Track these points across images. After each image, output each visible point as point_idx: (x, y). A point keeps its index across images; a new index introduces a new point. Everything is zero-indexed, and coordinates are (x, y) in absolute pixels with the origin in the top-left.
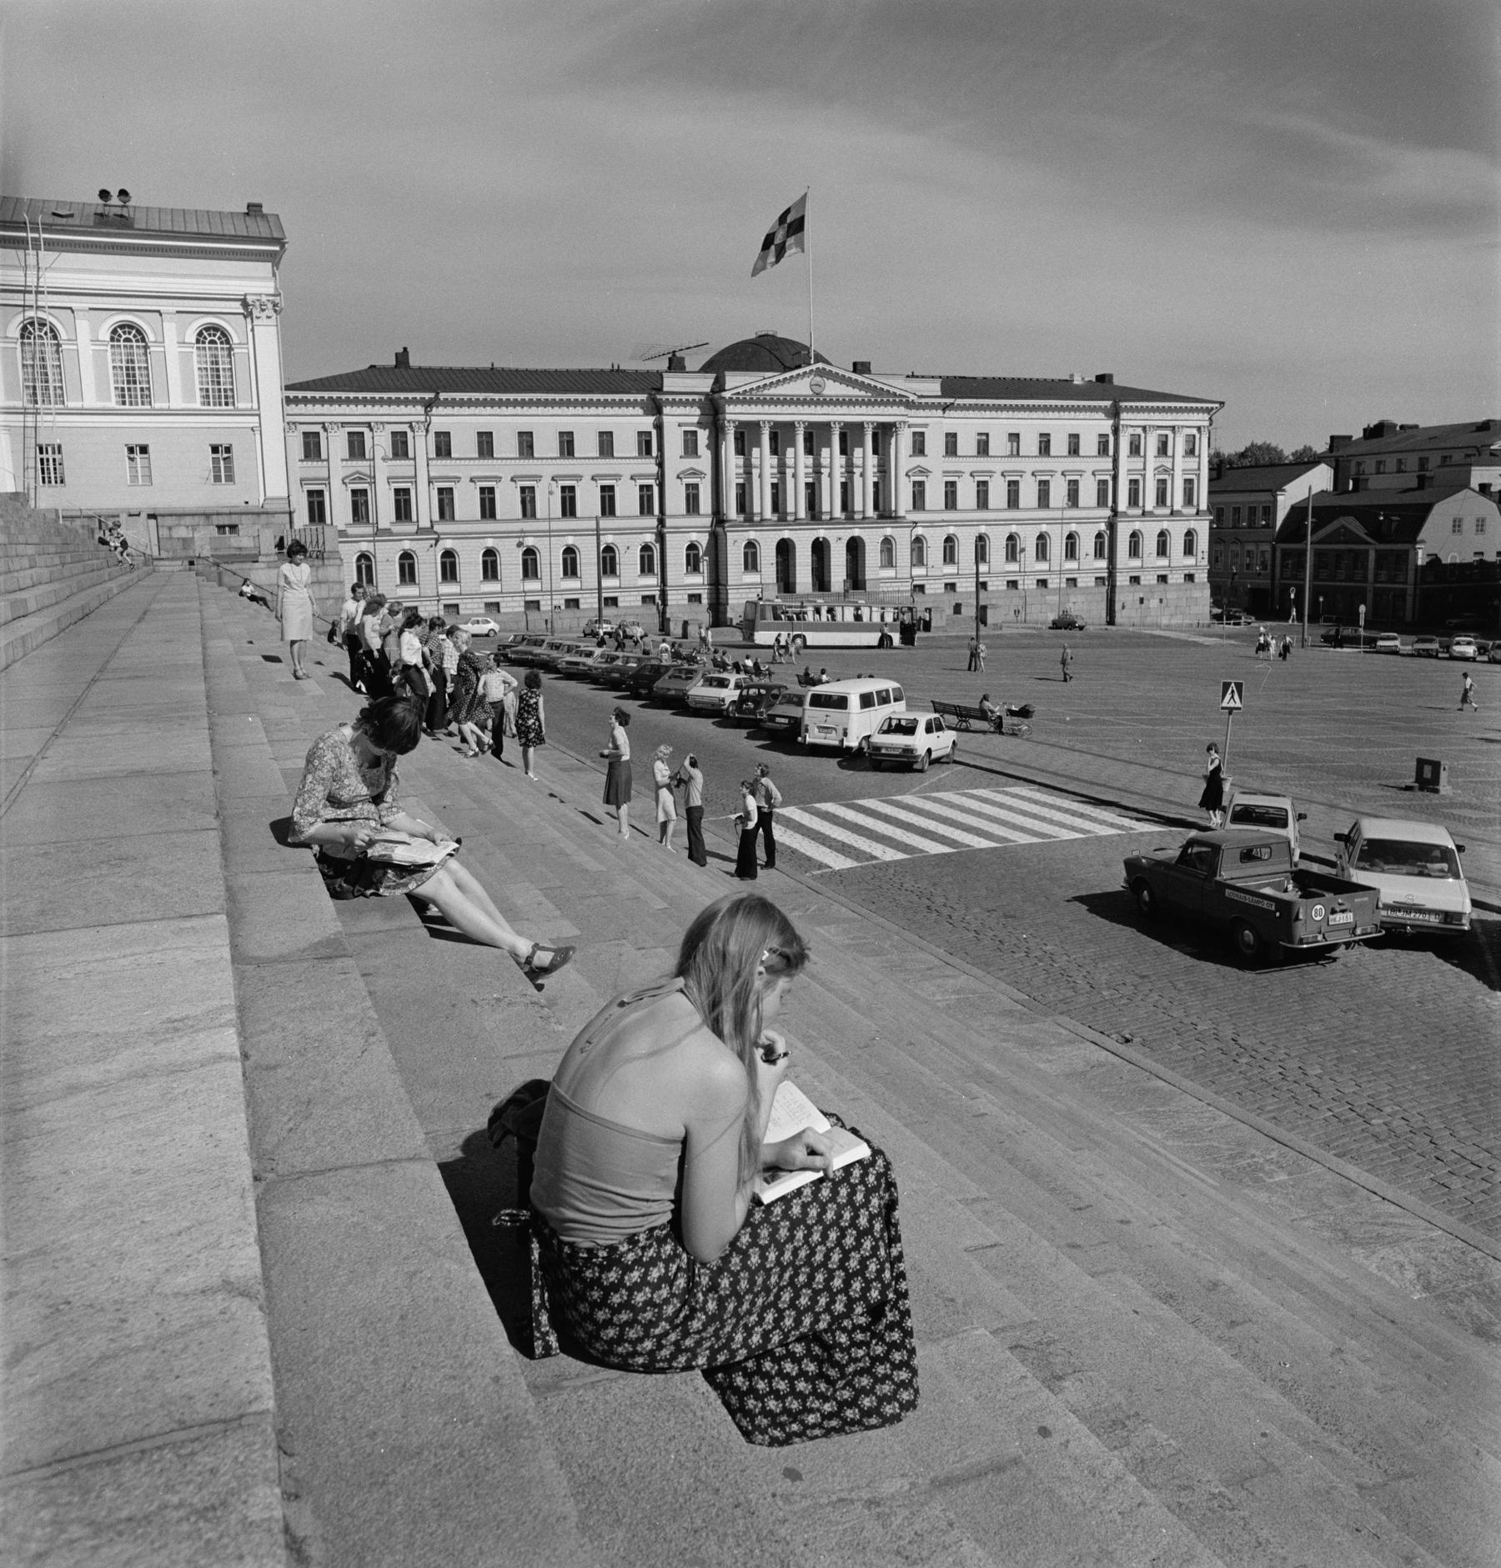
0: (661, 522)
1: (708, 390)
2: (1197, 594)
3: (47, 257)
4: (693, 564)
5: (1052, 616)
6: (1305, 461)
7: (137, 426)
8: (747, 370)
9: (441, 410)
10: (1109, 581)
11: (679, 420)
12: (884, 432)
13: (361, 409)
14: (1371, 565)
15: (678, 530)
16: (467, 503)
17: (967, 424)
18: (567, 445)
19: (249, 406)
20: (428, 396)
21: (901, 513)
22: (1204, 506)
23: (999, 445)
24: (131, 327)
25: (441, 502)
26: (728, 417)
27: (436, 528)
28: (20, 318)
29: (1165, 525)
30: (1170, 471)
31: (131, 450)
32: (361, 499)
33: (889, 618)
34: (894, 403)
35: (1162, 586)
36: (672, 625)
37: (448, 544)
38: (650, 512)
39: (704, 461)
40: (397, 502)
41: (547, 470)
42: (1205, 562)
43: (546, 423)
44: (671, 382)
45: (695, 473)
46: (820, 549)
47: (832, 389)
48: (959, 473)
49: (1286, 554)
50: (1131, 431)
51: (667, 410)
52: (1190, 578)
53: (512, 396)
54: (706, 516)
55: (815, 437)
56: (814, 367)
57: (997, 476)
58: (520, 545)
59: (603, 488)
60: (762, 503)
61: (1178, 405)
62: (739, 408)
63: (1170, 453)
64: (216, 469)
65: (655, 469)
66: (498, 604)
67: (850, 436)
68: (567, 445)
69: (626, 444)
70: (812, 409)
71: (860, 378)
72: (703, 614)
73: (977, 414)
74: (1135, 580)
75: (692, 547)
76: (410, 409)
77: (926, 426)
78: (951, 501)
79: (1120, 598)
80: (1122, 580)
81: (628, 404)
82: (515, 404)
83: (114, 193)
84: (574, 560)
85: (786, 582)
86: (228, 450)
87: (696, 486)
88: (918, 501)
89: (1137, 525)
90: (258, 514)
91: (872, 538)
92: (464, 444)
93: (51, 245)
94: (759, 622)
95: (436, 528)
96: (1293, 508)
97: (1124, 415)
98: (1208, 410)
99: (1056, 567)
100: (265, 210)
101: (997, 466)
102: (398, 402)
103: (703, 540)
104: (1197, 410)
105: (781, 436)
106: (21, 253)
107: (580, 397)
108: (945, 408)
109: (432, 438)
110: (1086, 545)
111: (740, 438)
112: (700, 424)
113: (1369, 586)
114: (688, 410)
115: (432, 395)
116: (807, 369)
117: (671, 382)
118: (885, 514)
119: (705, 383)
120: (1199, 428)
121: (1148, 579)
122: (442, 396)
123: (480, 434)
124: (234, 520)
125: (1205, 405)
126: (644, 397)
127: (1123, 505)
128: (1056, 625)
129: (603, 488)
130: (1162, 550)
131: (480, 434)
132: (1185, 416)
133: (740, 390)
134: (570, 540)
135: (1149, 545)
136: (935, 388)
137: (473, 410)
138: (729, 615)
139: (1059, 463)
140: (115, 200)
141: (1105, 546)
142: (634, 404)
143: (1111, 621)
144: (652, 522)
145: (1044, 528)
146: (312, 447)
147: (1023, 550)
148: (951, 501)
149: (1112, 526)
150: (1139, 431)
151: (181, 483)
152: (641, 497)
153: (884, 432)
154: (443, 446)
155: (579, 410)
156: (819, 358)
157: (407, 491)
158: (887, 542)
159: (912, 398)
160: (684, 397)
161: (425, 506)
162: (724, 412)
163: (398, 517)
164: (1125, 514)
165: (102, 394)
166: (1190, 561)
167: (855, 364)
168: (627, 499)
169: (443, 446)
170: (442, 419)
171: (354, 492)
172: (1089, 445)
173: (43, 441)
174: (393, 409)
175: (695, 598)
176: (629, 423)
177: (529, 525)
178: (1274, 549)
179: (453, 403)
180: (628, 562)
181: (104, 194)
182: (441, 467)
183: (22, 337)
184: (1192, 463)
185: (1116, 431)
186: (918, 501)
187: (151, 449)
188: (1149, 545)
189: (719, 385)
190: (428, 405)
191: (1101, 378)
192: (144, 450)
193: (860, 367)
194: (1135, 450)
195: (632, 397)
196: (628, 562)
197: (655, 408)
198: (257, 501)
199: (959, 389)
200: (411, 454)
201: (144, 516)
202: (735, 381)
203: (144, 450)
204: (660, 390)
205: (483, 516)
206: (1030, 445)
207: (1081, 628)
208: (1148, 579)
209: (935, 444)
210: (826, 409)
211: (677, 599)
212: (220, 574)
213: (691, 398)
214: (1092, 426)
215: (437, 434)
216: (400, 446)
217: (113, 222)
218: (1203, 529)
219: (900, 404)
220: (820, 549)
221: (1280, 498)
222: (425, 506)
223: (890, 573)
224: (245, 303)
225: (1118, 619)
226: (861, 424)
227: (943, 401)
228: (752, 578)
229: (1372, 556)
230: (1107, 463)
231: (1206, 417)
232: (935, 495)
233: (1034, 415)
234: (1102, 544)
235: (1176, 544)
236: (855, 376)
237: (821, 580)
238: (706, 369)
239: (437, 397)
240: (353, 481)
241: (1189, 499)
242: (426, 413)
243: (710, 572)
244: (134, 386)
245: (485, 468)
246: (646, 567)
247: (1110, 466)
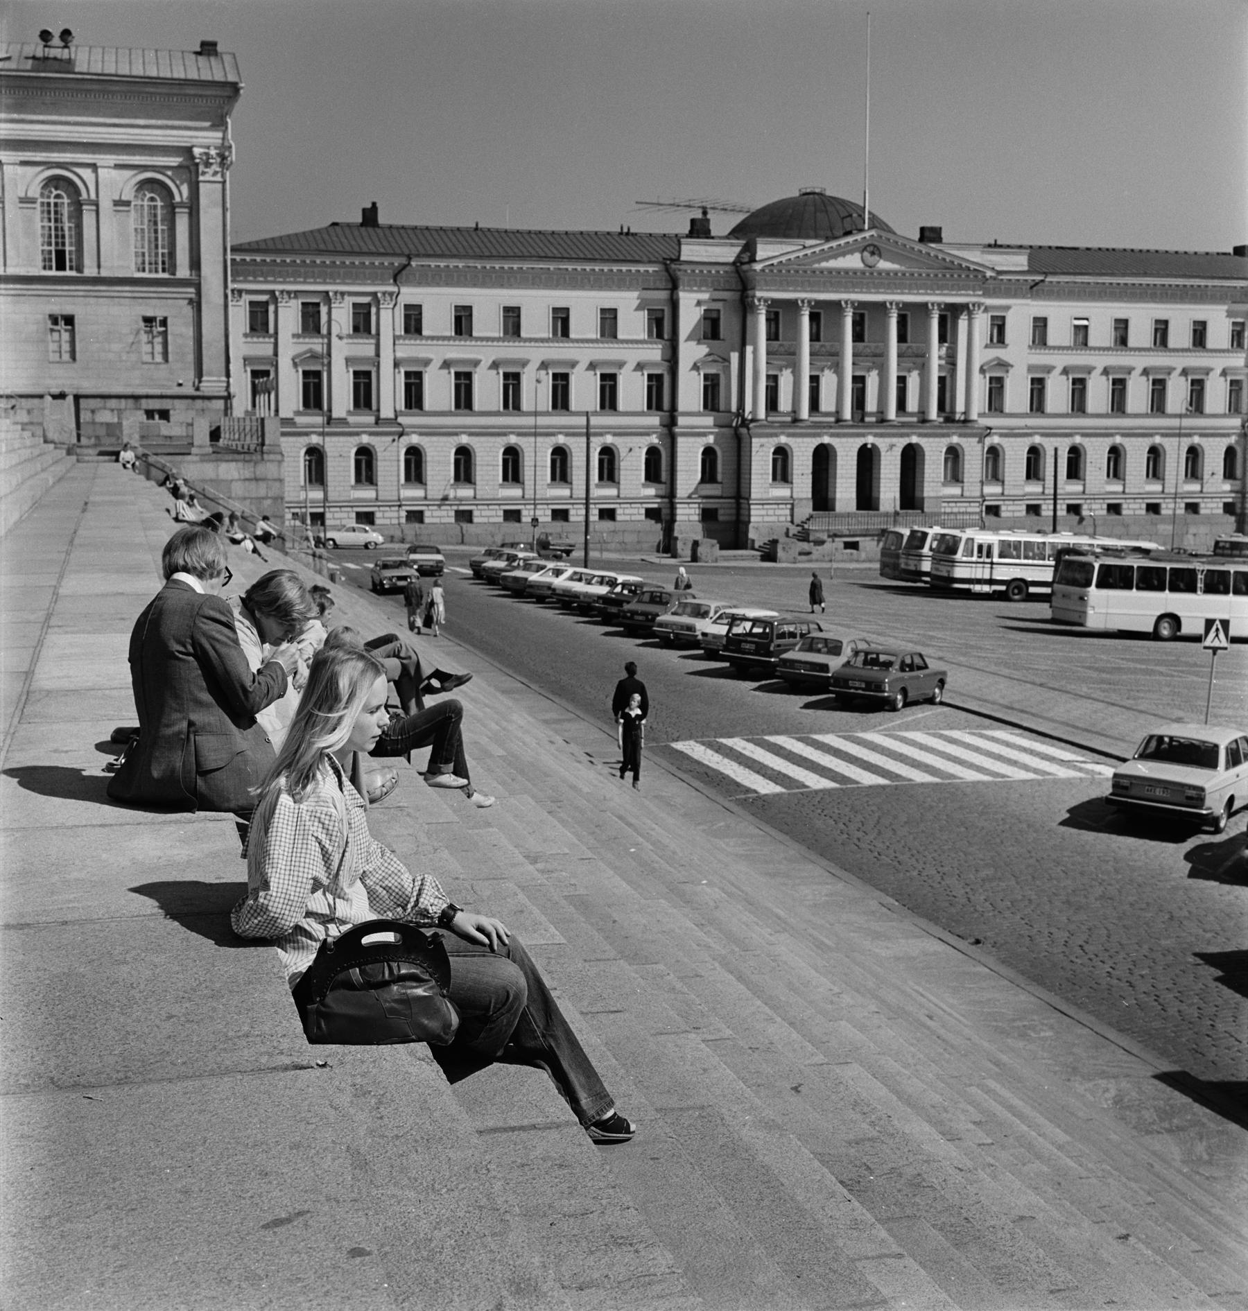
8: (786, 236)
16: (438, 390)
21: (974, 416)
26: (759, 294)
27: (400, 420)
36: (679, 545)
46: (867, 460)
85: (822, 499)
91: (934, 451)
92: (437, 319)
95: (400, 420)
99: (1170, 489)
111: (773, 320)
117: (692, 251)
136: (1020, 261)
138: (751, 535)
146: (260, 321)
154: (413, 322)
156: (876, 223)
157: (368, 374)
158: (954, 454)
167: (922, 230)
168: (632, 390)
169: (413, 322)
180: (632, 466)
182: (411, 349)
193: (930, 235)
201: (70, 399)
204: (677, 260)
215: (406, 306)
216: (363, 323)
220: (867, 460)
223: (955, 490)
226: (925, 305)
228: (782, 492)
232: (1017, 394)
237: (867, 498)
238: (737, 232)
240: (304, 361)
245: (460, 351)
246: (652, 474)
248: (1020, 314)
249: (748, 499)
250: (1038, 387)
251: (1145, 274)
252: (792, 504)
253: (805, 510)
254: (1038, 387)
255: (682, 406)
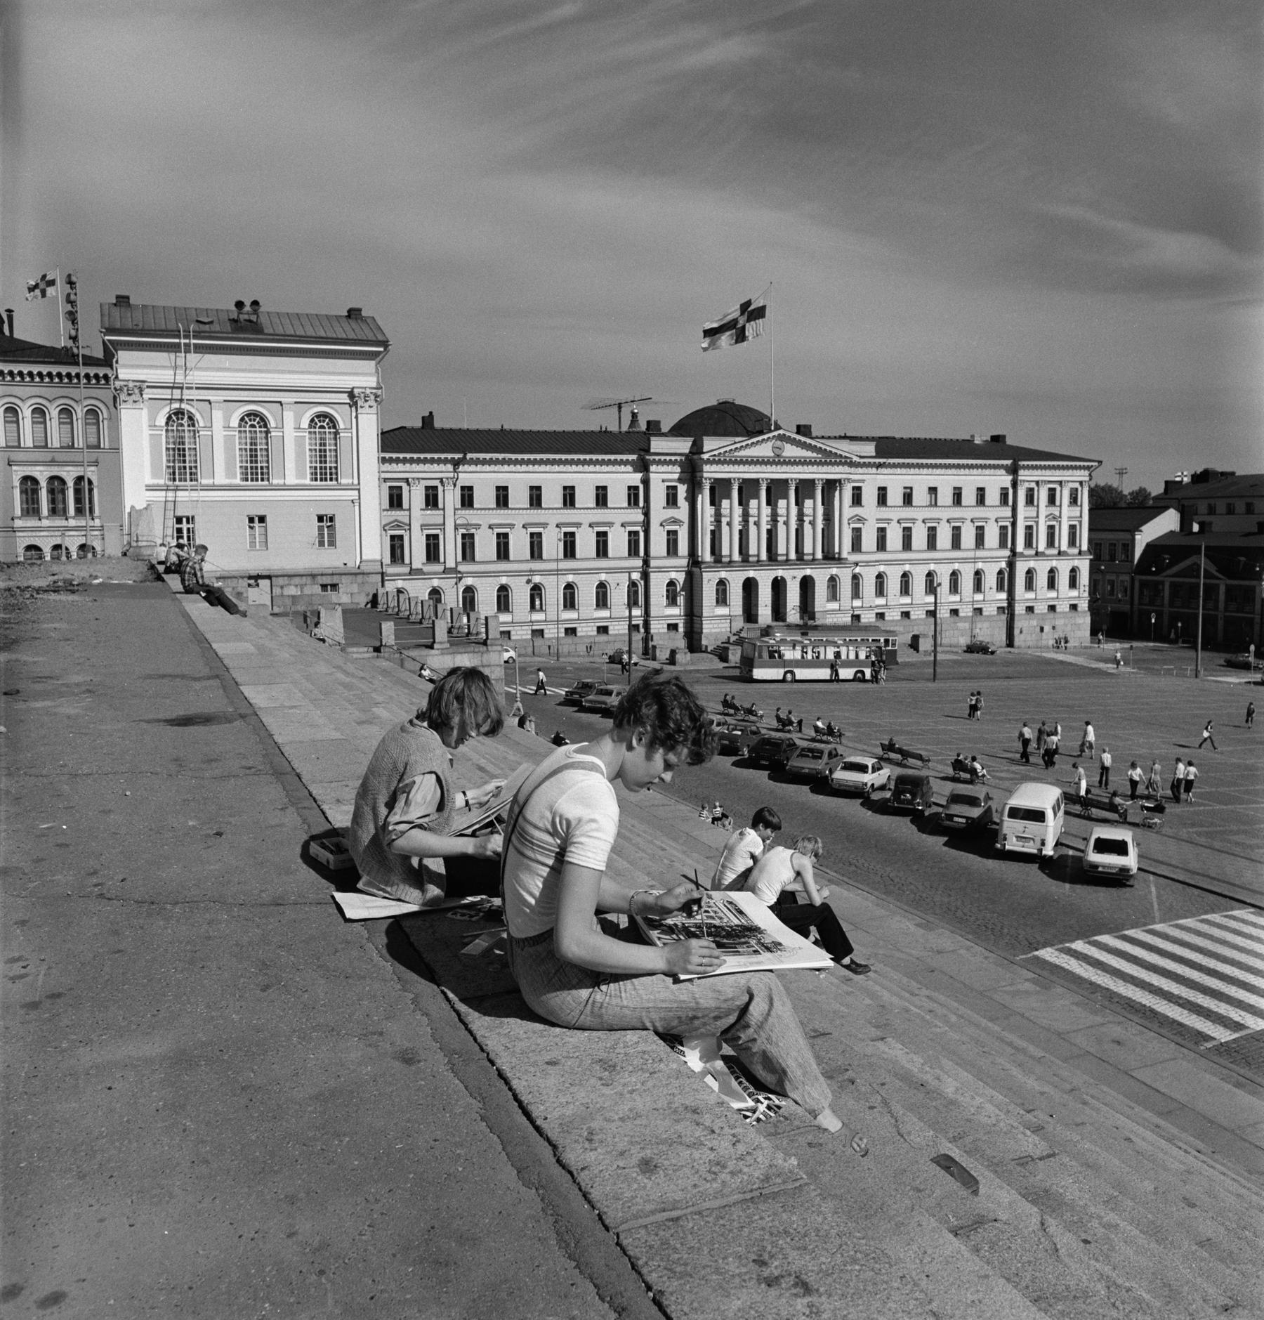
0: (646, 562)
1: (687, 451)
2: (1080, 621)
3: (193, 358)
4: (672, 600)
5: (964, 641)
6: (1157, 508)
7: (257, 499)
9: (466, 468)
10: (1009, 610)
11: (663, 477)
12: (831, 486)
13: (401, 467)
14: (1222, 597)
15: (660, 570)
16: (485, 546)
17: (895, 480)
18: (569, 496)
19: (350, 481)
20: (457, 456)
21: (844, 555)
22: (1085, 547)
23: (920, 497)
24: (256, 415)
25: (464, 545)
26: (705, 475)
28: (167, 409)
29: (1054, 563)
30: (1058, 518)
31: (251, 520)
32: (397, 543)
33: (862, 656)
34: (840, 463)
35: (1052, 615)
37: (469, 581)
38: (636, 554)
39: (682, 512)
40: (428, 546)
41: (552, 518)
42: (1086, 594)
43: (552, 479)
44: (657, 445)
45: (676, 521)
46: (778, 586)
47: (790, 451)
48: (888, 521)
49: (1143, 585)
50: (1027, 485)
51: (653, 468)
52: (1074, 607)
53: (526, 457)
54: (684, 557)
55: (776, 490)
56: (776, 433)
57: (919, 523)
58: (529, 581)
59: (598, 534)
60: (730, 546)
61: (1065, 463)
62: (714, 468)
63: (1058, 503)
64: (321, 535)
65: (641, 518)
66: (509, 632)
67: (804, 489)
68: (569, 496)
69: (617, 497)
70: (774, 468)
71: (803, 439)
72: (679, 641)
73: (904, 471)
74: (1030, 609)
75: (671, 584)
76: (442, 467)
77: (863, 481)
78: (882, 545)
79: (1018, 624)
80: (1019, 609)
81: (621, 463)
82: (528, 462)
83: (248, 303)
84: (573, 595)
85: (750, 614)
86: (331, 519)
87: (675, 532)
88: (856, 546)
89: (1032, 564)
90: (356, 574)
91: (821, 576)
92: (485, 497)
93: (199, 349)
94: (757, 661)
96: (1148, 546)
97: (1021, 472)
98: (1088, 468)
100: (363, 314)
101: (919, 514)
102: (432, 461)
103: (680, 577)
104: (1080, 468)
105: (748, 489)
106: (172, 355)
107: (582, 457)
108: (879, 466)
109: (458, 492)
110: (990, 580)
112: (680, 480)
113: (1220, 615)
114: (670, 468)
115: (461, 456)
116: (771, 435)
117: (657, 445)
118: (830, 556)
119: (683, 445)
120: (1081, 483)
121: (1041, 608)
122: (469, 456)
123: (498, 488)
124: (335, 580)
125: (1086, 464)
126: (634, 457)
127: (1020, 547)
128: (970, 649)
129: (598, 534)
130: (1052, 584)
131: (498, 488)
132: (1070, 472)
133: (716, 453)
134: (570, 578)
135: (1041, 580)
136: (870, 449)
137: (493, 468)
138: (704, 642)
139: (969, 511)
140: (248, 308)
141: (1006, 581)
142: (626, 463)
143: (1010, 643)
144: (638, 563)
145: (956, 566)
147: (939, 585)
148: (882, 545)
149: (1011, 565)
150: (1033, 485)
151: (294, 550)
152: (630, 541)
153: (831, 486)
154: (467, 498)
155: (580, 468)
157: (436, 537)
159: (855, 459)
160: (668, 458)
161: (451, 550)
162: (702, 471)
163: (429, 558)
164: (1022, 555)
165: (230, 473)
166: (1074, 593)
168: (618, 542)
169: (467, 498)
170: (467, 476)
171: (393, 537)
172: (993, 497)
173: (179, 514)
174: (428, 467)
175: (672, 627)
176: (620, 478)
177: (537, 565)
178: (1133, 579)
179: (477, 462)
180: (618, 596)
181: (240, 305)
183: (167, 424)
184: (1075, 511)
185: (1015, 484)
186: (856, 546)
187: (268, 519)
188: (1041, 580)
189: (697, 449)
190: (456, 464)
191: (997, 439)
192: (262, 519)
194: (1030, 500)
195: (624, 457)
196: (618, 596)
197: (643, 467)
198: (353, 562)
199: (892, 449)
200: (440, 506)
202: (711, 445)
203: (262, 519)
204: (647, 451)
205: (499, 557)
206: (945, 497)
207: (993, 653)
208: (1041, 608)
209: (869, 496)
210: (785, 468)
211: (658, 627)
212: (402, 660)
213: (673, 458)
214: (995, 481)
216: (432, 499)
217: (245, 328)
218: (1084, 566)
219: (845, 464)
220: (778, 586)
221: (1138, 537)
222: (451, 550)
223: (835, 606)
224: (351, 394)
225: (1017, 643)
226: (813, 480)
227: (877, 461)
228: (723, 611)
229: (1222, 589)
230: (1007, 512)
231: (1087, 473)
232: (869, 540)
233: (949, 471)
234: (1002, 579)
235: (1063, 579)
236: (798, 437)
239: (465, 457)
240: (393, 528)
241: (1072, 542)
242: (455, 471)
243: (686, 606)
244: (257, 469)
245: (501, 516)
246: (632, 602)
247: (1009, 514)
248: (871, 481)
249: (701, 616)
250: (882, 533)
251: (948, 458)
252: (731, 617)
253: (739, 623)
254: (882, 533)
255: (654, 551)
